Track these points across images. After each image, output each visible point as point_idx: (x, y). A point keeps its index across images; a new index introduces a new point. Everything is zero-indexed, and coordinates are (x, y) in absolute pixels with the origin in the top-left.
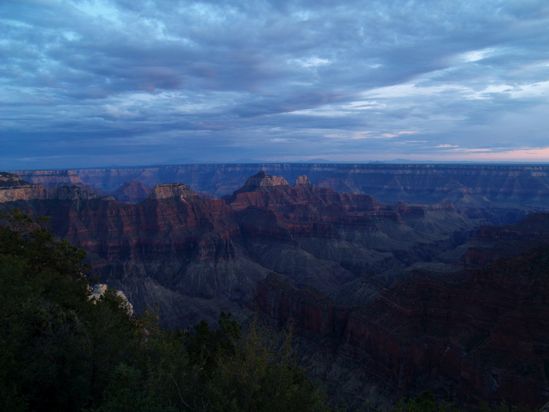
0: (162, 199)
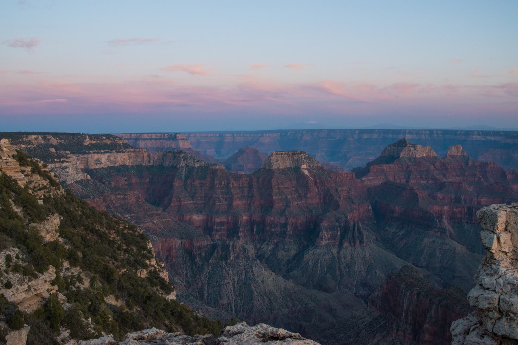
0: (279, 170)
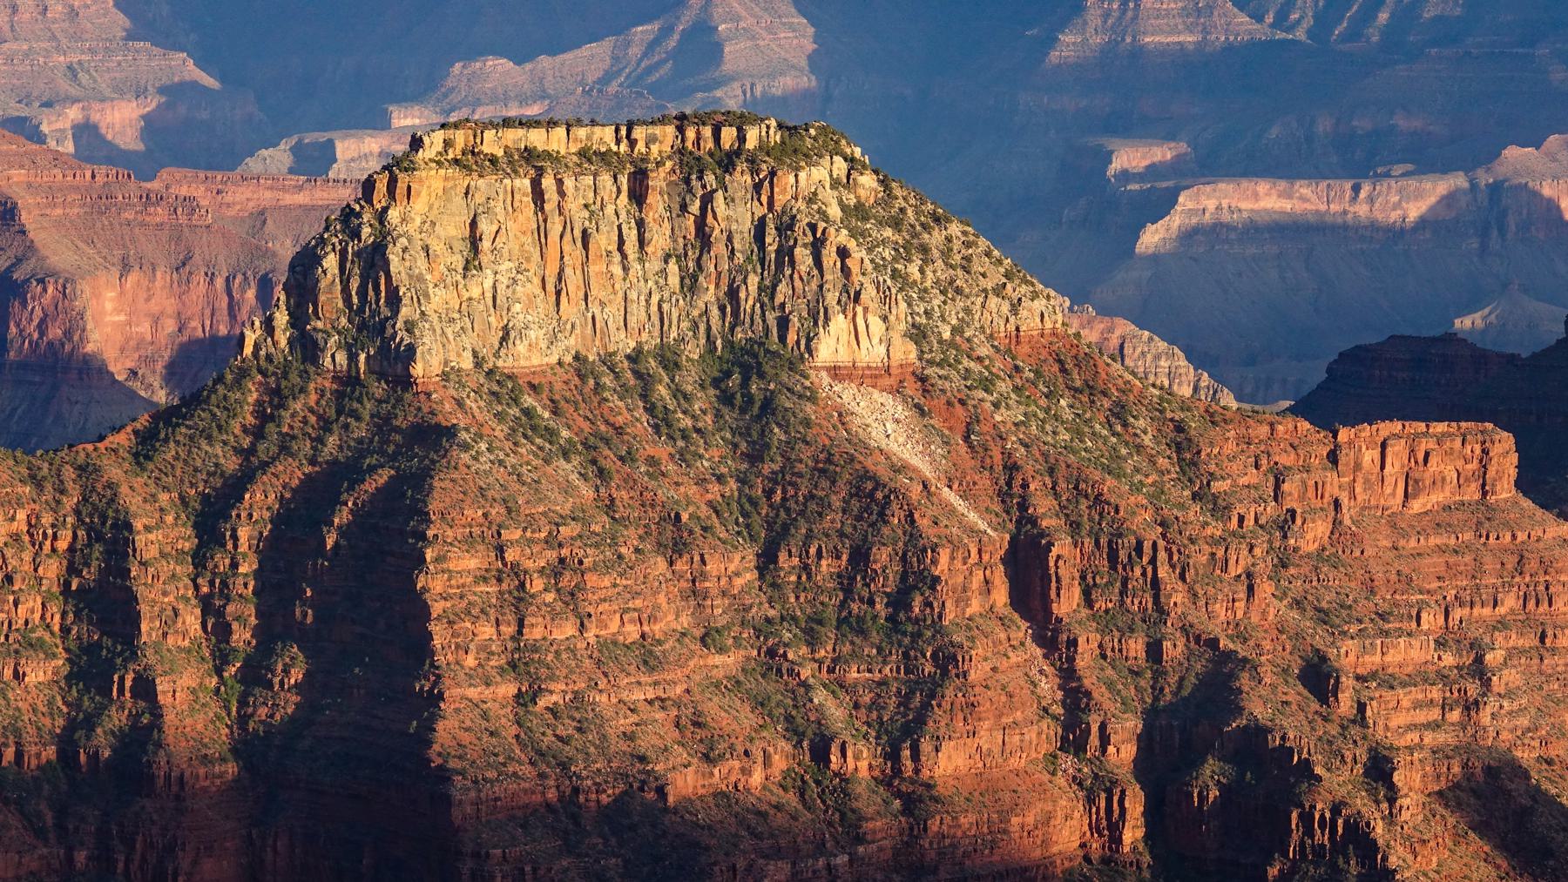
0: (503, 387)
